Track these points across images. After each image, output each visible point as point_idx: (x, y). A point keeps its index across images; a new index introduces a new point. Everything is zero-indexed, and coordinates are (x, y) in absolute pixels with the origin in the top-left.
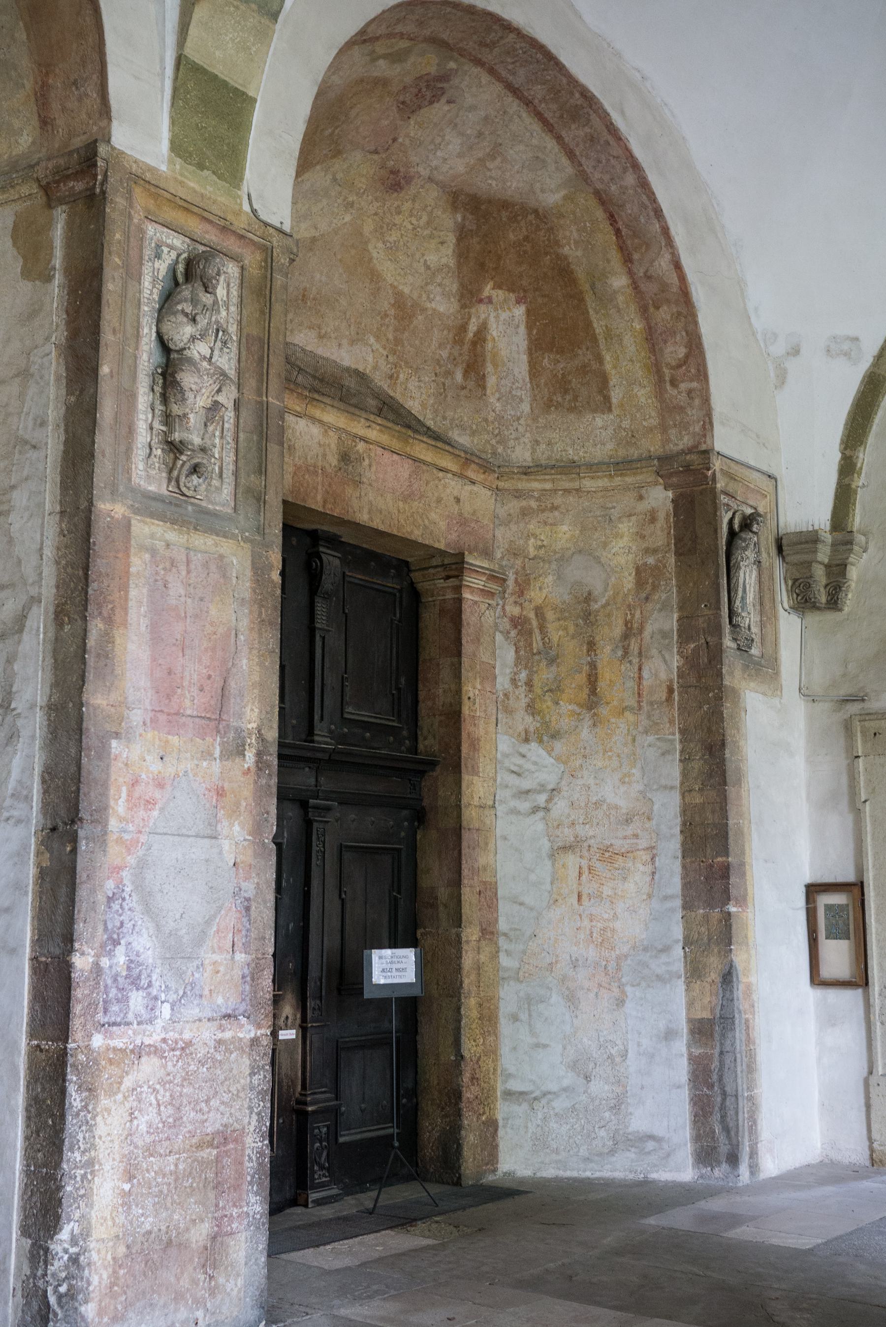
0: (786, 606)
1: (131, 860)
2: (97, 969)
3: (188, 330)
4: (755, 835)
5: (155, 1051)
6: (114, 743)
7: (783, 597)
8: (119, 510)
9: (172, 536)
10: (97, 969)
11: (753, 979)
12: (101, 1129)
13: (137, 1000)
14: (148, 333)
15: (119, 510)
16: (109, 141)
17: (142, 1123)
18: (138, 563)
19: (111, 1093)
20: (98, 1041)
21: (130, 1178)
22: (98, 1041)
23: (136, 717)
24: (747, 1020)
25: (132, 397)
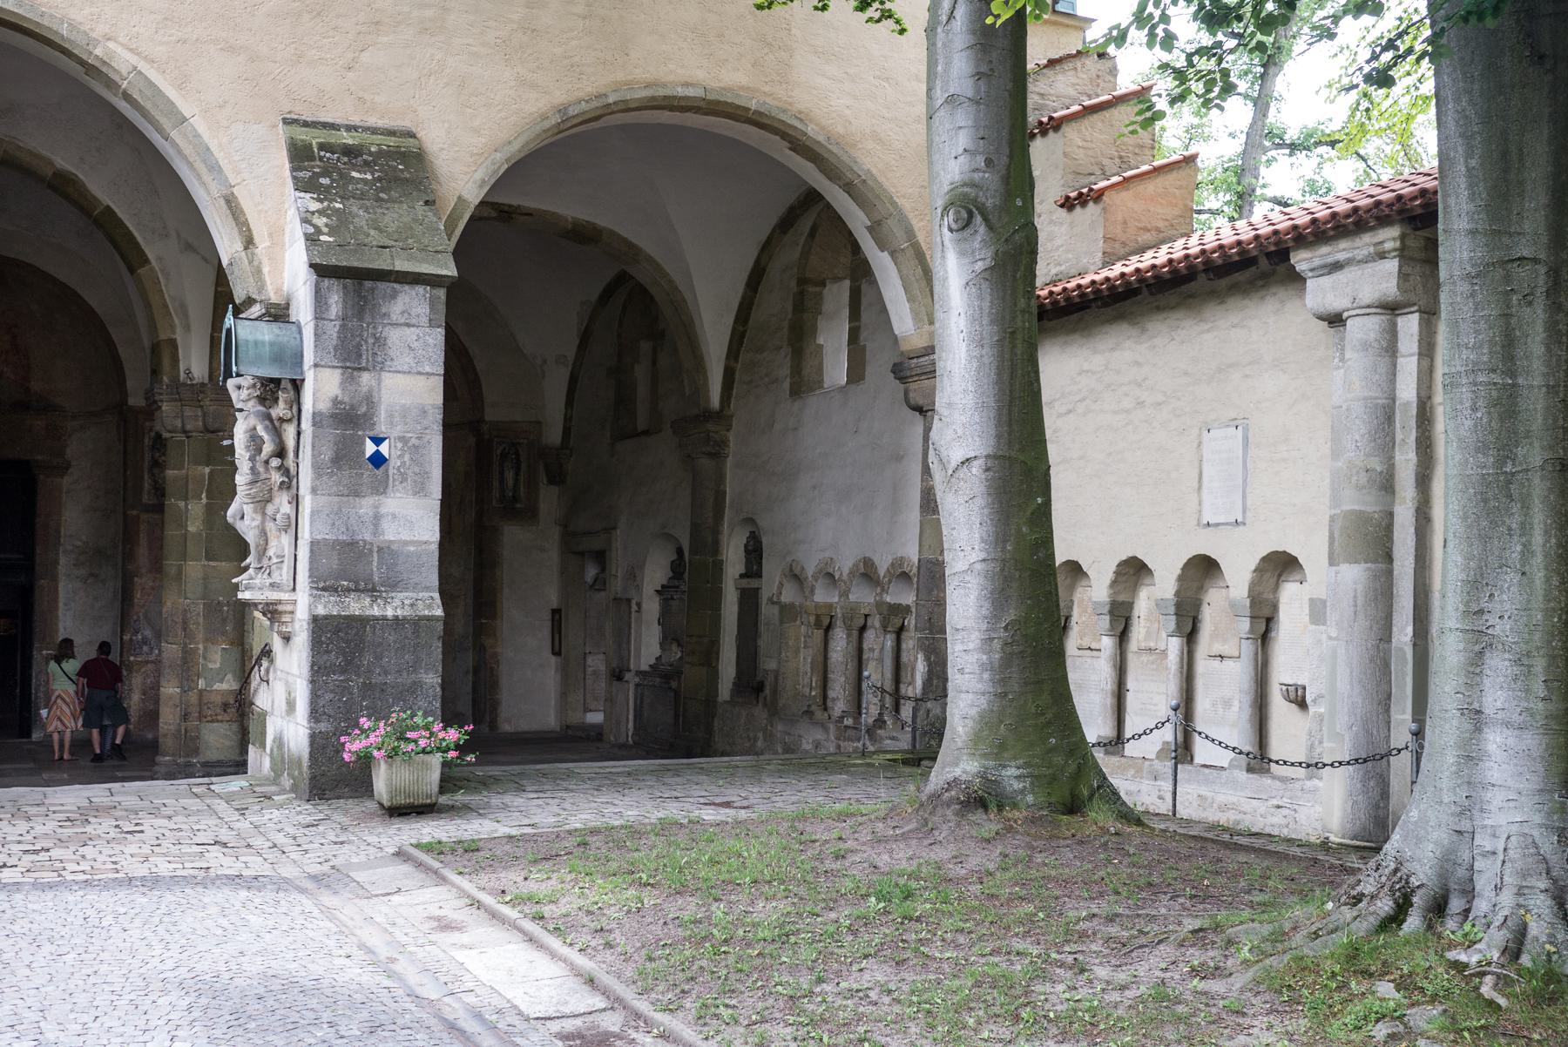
0: (545, 482)
1: (143, 610)
2: (131, 639)
3: (158, 454)
4: (506, 591)
5: (152, 662)
6: (136, 579)
7: (543, 477)
8: (135, 512)
9: (156, 516)
10: (131, 639)
11: (499, 650)
12: (134, 681)
13: (145, 648)
14: (147, 456)
15: (135, 512)
16: (126, 404)
17: (149, 681)
18: (143, 527)
19: (137, 672)
20: (132, 658)
21: (144, 695)
22: (132, 658)
23: (144, 571)
24: (492, 669)
25: (142, 478)
